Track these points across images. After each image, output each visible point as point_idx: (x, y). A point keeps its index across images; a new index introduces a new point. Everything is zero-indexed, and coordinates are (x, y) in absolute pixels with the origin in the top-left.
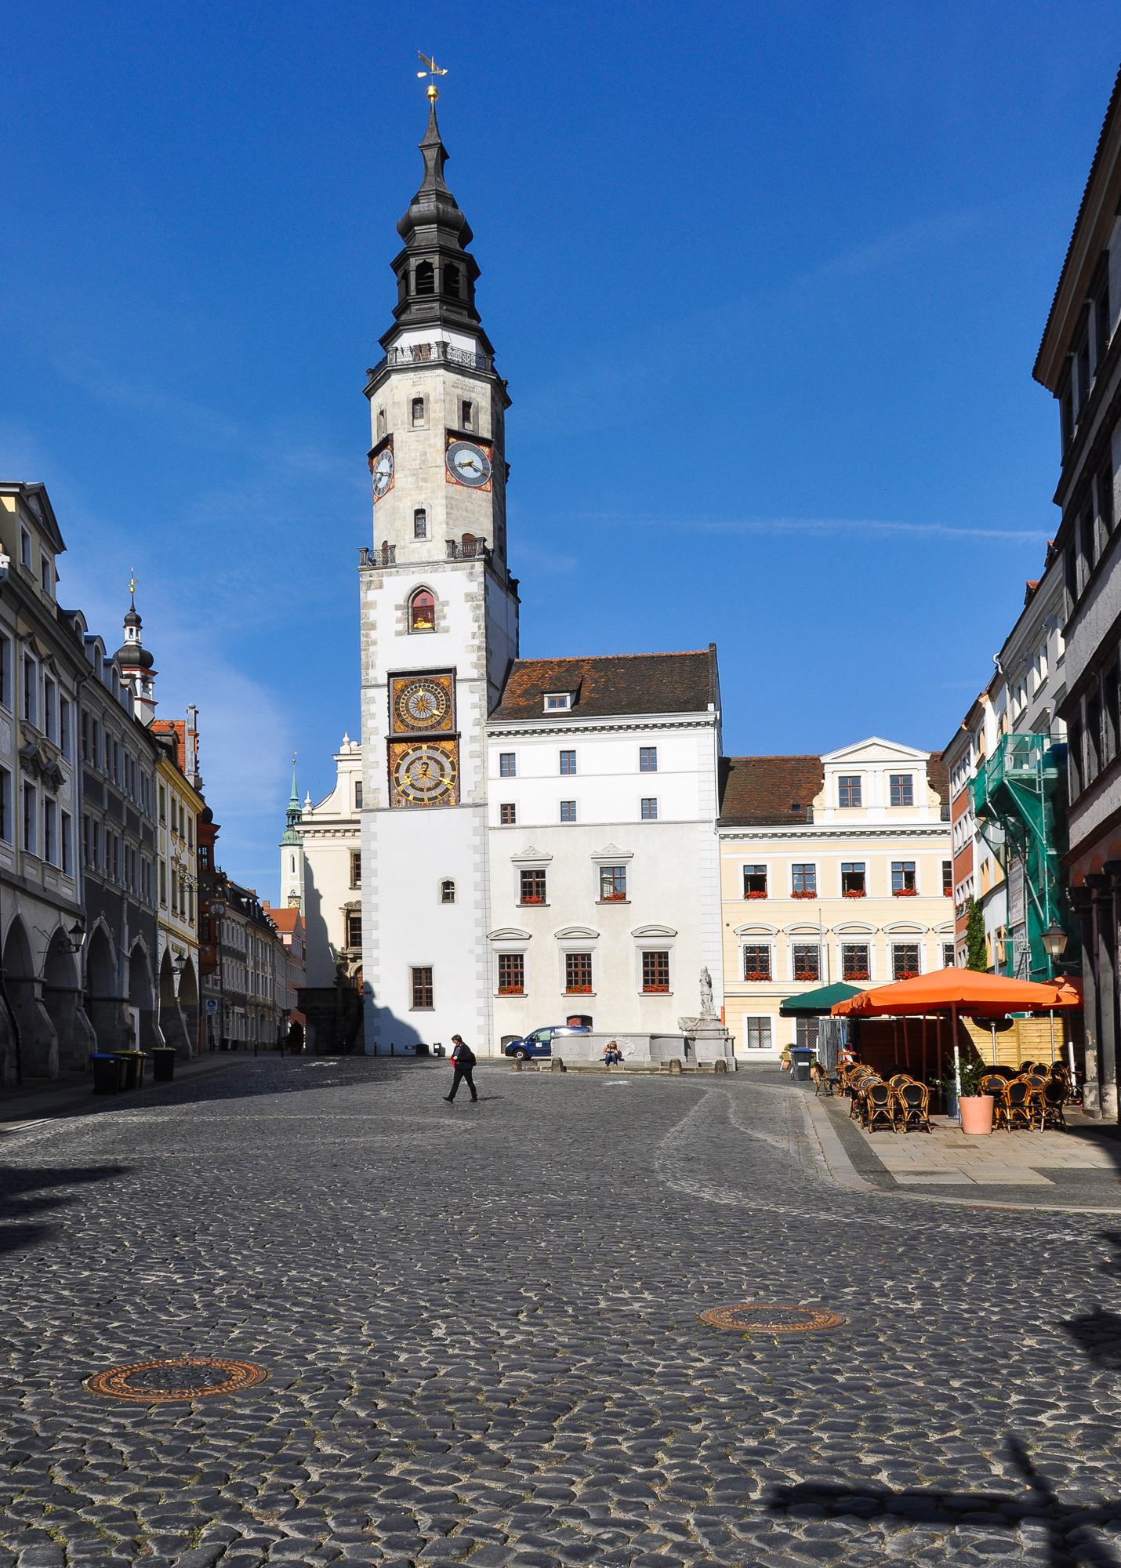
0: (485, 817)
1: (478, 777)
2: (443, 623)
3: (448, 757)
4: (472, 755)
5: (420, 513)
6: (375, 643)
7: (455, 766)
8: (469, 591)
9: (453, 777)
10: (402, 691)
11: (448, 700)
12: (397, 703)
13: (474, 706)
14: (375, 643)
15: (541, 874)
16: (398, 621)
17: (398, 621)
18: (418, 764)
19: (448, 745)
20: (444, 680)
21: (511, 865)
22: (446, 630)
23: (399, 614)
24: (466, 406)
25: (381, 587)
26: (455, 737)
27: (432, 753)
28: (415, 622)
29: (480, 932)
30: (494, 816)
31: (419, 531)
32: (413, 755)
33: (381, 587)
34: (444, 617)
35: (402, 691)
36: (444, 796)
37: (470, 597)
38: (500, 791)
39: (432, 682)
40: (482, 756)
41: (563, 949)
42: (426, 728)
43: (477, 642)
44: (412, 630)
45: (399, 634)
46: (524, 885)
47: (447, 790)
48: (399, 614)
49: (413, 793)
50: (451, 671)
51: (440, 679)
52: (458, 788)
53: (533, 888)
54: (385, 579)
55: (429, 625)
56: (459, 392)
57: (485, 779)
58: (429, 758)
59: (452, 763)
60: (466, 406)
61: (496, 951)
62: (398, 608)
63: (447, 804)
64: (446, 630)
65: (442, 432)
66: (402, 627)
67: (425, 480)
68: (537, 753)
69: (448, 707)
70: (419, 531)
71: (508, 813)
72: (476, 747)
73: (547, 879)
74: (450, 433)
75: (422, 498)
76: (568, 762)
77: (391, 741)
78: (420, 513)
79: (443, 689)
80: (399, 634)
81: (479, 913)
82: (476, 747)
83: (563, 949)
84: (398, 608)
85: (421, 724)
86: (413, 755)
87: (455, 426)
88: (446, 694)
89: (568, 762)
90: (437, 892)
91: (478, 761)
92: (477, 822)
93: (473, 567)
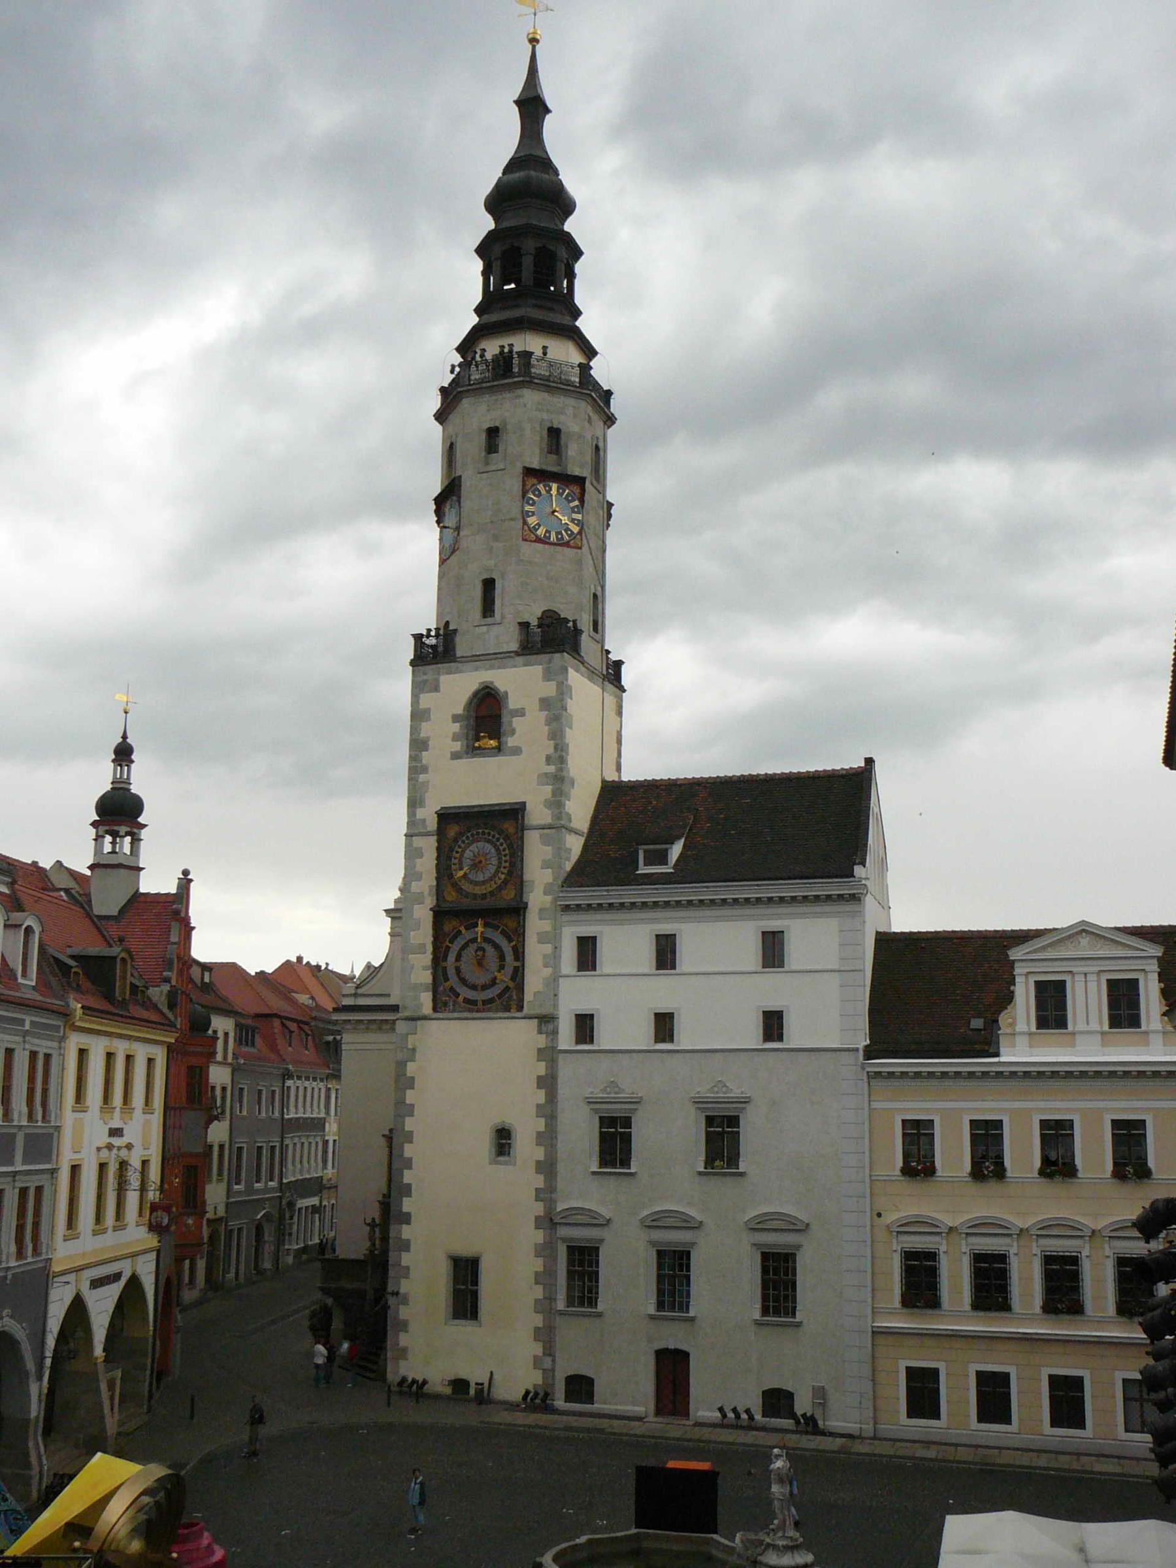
0: (555, 1032)
1: (548, 971)
2: (511, 742)
3: (510, 940)
4: (543, 938)
5: (489, 585)
6: (425, 769)
7: (519, 954)
8: (544, 695)
9: (516, 970)
10: (456, 840)
11: (512, 855)
12: (449, 858)
13: (546, 865)
14: (425, 769)
15: (627, 1122)
16: (455, 738)
17: (455, 738)
18: (472, 948)
19: (511, 924)
20: (509, 826)
21: (585, 1110)
22: (517, 751)
23: (456, 727)
24: (554, 434)
25: (436, 689)
26: (518, 910)
27: (491, 934)
28: (478, 739)
29: (539, 1209)
30: (566, 1036)
31: (488, 608)
32: (467, 935)
33: (436, 689)
34: (513, 732)
35: (456, 840)
36: (506, 998)
37: (545, 703)
38: (577, 994)
39: (494, 828)
40: (553, 938)
41: (652, 1243)
42: (484, 897)
43: (552, 769)
44: (472, 750)
45: (455, 756)
46: (603, 1137)
47: (507, 988)
48: (456, 727)
49: (465, 993)
50: (514, 813)
51: (502, 823)
52: (520, 988)
53: (615, 1142)
54: (443, 679)
55: (493, 743)
56: (545, 416)
57: (556, 978)
58: (487, 940)
59: (515, 949)
60: (554, 434)
61: (564, 1240)
62: (456, 718)
63: (507, 1009)
64: (517, 751)
65: (519, 469)
66: (457, 746)
67: (496, 538)
68: (626, 943)
69: (512, 864)
70: (488, 608)
71: (585, 1026)
72: (546, 926)
73: (634, 1130)
74: (529, 472)
75: (492, 563)
76: (666, 954)
77: (440, 915)
78: (489, 585)
79: (507, 838)
80: (455, 756)
81: (540, 1181)
82: (546, 926)
83: (652, 1243)
84: (456, 718)
85: (478, 890)
86: (467, 935)
87: (535, 464)
88: (510, 847)
89: (666, 954)
90: (485, 1144)
91: (548, 948)
92: (542, 1041)
93: (550, 661)
